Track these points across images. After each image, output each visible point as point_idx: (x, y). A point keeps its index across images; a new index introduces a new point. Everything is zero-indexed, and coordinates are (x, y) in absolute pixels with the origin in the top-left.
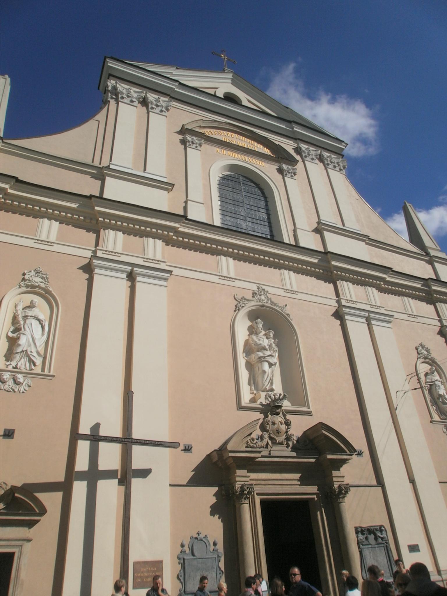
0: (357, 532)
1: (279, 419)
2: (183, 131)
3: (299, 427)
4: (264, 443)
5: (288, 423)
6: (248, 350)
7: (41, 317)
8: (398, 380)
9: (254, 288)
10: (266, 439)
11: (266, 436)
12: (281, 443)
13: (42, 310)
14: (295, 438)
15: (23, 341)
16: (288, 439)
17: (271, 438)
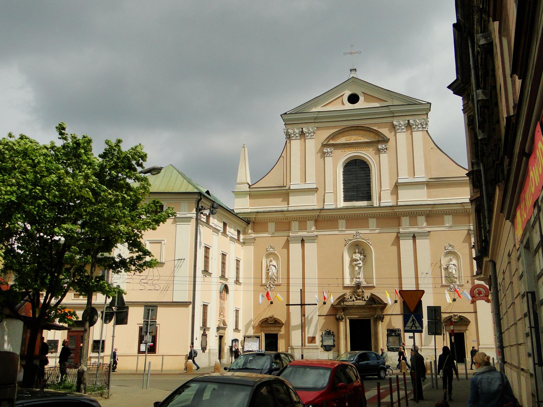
0: (387, 331)
1: (360, 290)
2: (324, 145)
3: (367, 294)
4: (352, 300)
5: (363, 292)
6: (353, 260)
7: (275, 263)
8: (425, 266)
9: (354, 232)
10: (354, 298)
11: (354, 297)
12: (360, 299)
13: (274, 263)
14: (366, 297)
15: (270, 274)
16: (363, 297)
17: (356, 297)
